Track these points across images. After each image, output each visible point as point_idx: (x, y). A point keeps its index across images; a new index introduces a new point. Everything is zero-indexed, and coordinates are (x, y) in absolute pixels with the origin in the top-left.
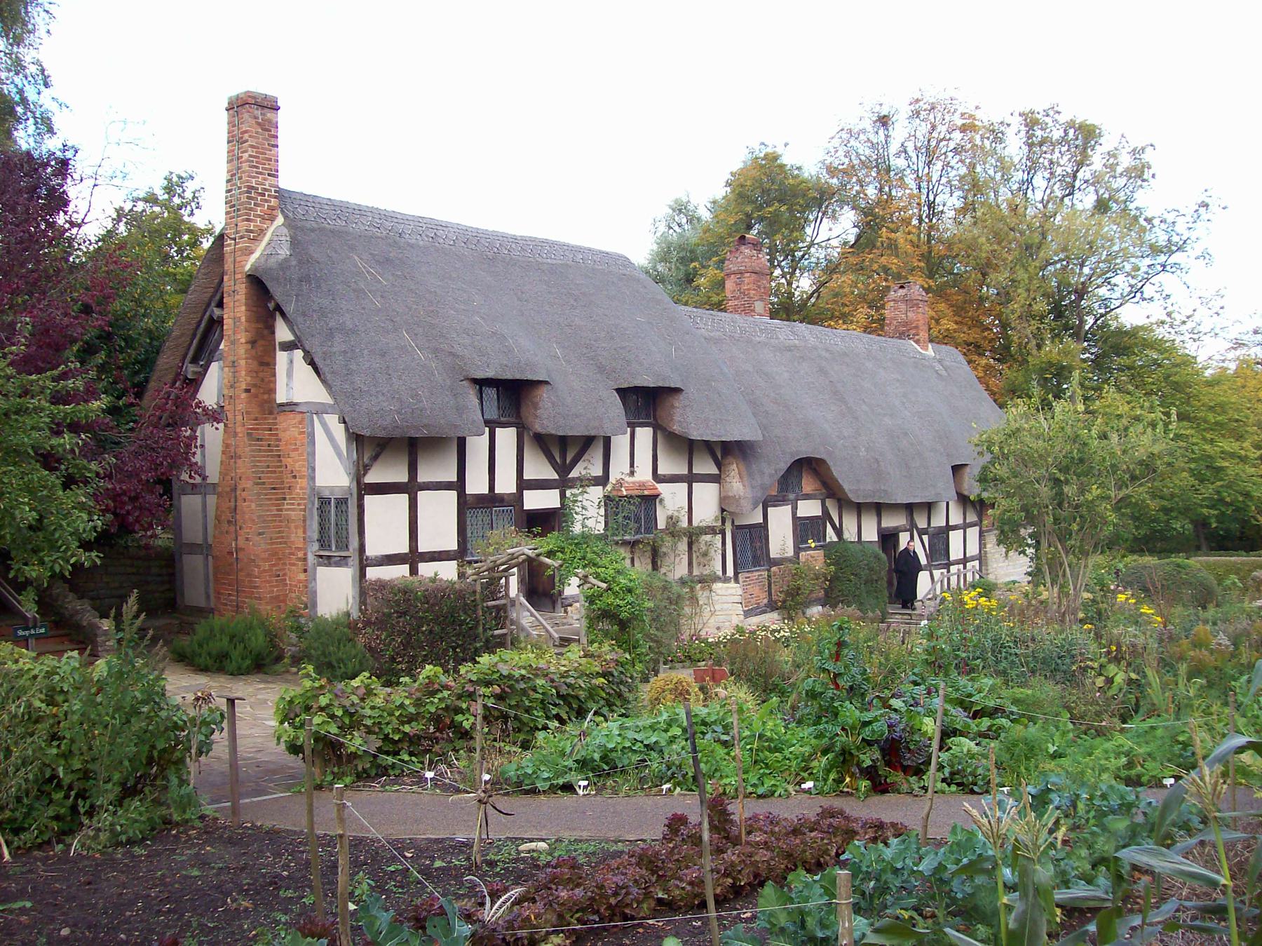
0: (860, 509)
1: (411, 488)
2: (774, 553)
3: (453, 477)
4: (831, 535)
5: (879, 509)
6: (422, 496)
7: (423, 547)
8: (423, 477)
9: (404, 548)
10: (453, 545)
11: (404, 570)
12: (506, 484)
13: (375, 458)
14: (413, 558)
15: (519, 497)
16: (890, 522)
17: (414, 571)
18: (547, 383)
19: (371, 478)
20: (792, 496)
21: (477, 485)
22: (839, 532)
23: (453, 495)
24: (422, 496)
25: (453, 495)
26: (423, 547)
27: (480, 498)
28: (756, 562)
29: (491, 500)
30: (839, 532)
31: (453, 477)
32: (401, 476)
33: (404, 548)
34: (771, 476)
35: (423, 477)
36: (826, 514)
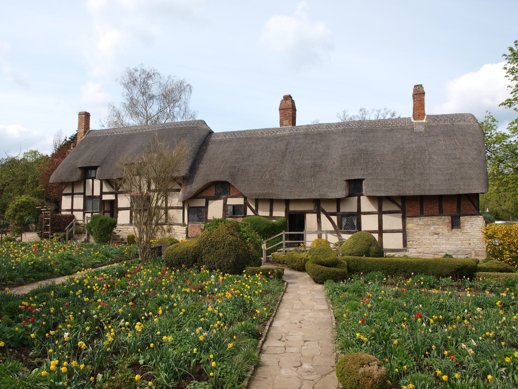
0: (272, 202)
1: (72, 195)
2: (210, 217)
3: (83, 192)
4: (249, 212)
5: (287, 202)
6: (74, 196)
7: (74, 208)
8: (75, 192)
9: (70, 208)
10: (82, 208)
11: (70, 213)
12: (97, 193)
13: (65, 188)
14: (72, 210)
15: (101, 196)
16: (293, 208)
17: (72, 213)
18: (99, 166)
19: (64, 192)
20: (224, 196)
21: (89, 193)
22: (255, 212)
23: (83, 196)
24: (74, 196)
25: (83, 196)
26: (74, 208)
27: (89, 197)
28: (200, 220)
29: (93, 197)
30: (255, 212)
31: (83, 192)
32: (70, 192)
33: (70, 208)
34: (195, 188)
35: (75, 192)
36: (246, 204)
